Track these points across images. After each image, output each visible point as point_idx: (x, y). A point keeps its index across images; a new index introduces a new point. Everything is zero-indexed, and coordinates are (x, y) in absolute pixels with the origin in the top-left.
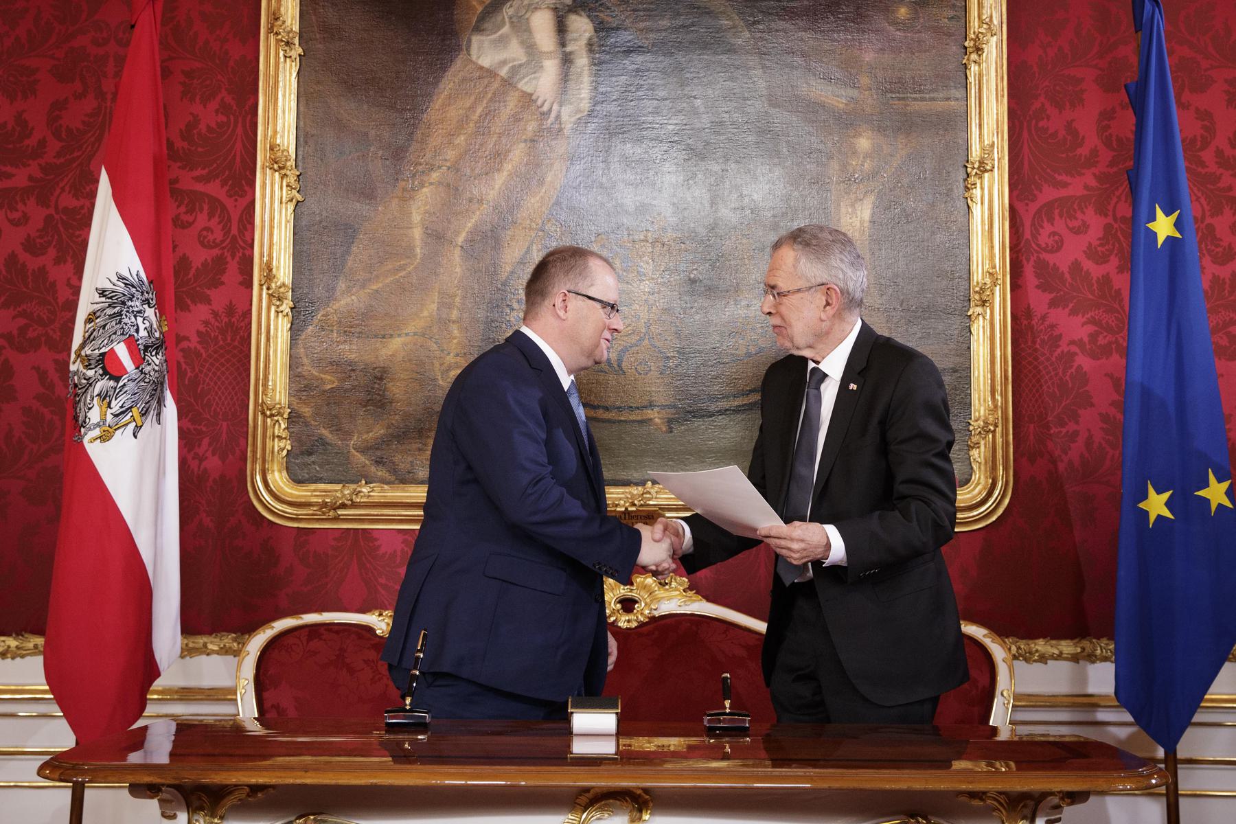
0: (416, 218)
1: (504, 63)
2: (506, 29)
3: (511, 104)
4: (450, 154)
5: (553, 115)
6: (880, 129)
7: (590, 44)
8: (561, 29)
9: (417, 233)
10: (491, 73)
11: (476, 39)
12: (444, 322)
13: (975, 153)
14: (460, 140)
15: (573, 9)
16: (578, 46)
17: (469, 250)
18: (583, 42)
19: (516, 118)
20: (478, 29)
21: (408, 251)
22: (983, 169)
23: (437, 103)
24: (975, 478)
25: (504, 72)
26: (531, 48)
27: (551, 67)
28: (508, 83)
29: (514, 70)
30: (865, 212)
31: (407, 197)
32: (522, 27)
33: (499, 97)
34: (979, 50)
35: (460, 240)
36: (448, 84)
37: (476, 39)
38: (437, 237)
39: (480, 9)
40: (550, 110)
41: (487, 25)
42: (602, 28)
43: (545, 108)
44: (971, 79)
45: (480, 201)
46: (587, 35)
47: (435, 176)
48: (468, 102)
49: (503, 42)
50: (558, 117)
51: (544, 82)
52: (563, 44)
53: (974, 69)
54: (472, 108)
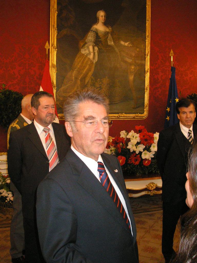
0: (73, 75)
1: (85, 53)
2: (86, 48)
3: (87, 59)
5: (92, 61)
7: (97, 51)
9: (74, 78)
10: (83, 55)
11: (82, 49)
14: (80, 64)
15: (95, 46)
16: (96, 52)
18: (96, 51)
20: (82, 48)
21: (72, 80)
23: (76, 58)
24: (145, 113)
25: (86, 55)
26: (89, 51)
27: (92, 54)
28: (86, 56)
29: (87, 54)
32: (88, 48)
35: (80, 79)
36: (78, 55)
37: (82, 49)
38: (76, 78)
39: (82, 45)
40: (92, 61)
42: (99, 49)
43: (91, 60)
44: (146, 59)
45: (82, 73)
46: (97, 50)
47: (76, 69)
48: (80, 59)
49: (85, 50)
50: (93, 61)
51: (91, 56)
54: (81, 60)
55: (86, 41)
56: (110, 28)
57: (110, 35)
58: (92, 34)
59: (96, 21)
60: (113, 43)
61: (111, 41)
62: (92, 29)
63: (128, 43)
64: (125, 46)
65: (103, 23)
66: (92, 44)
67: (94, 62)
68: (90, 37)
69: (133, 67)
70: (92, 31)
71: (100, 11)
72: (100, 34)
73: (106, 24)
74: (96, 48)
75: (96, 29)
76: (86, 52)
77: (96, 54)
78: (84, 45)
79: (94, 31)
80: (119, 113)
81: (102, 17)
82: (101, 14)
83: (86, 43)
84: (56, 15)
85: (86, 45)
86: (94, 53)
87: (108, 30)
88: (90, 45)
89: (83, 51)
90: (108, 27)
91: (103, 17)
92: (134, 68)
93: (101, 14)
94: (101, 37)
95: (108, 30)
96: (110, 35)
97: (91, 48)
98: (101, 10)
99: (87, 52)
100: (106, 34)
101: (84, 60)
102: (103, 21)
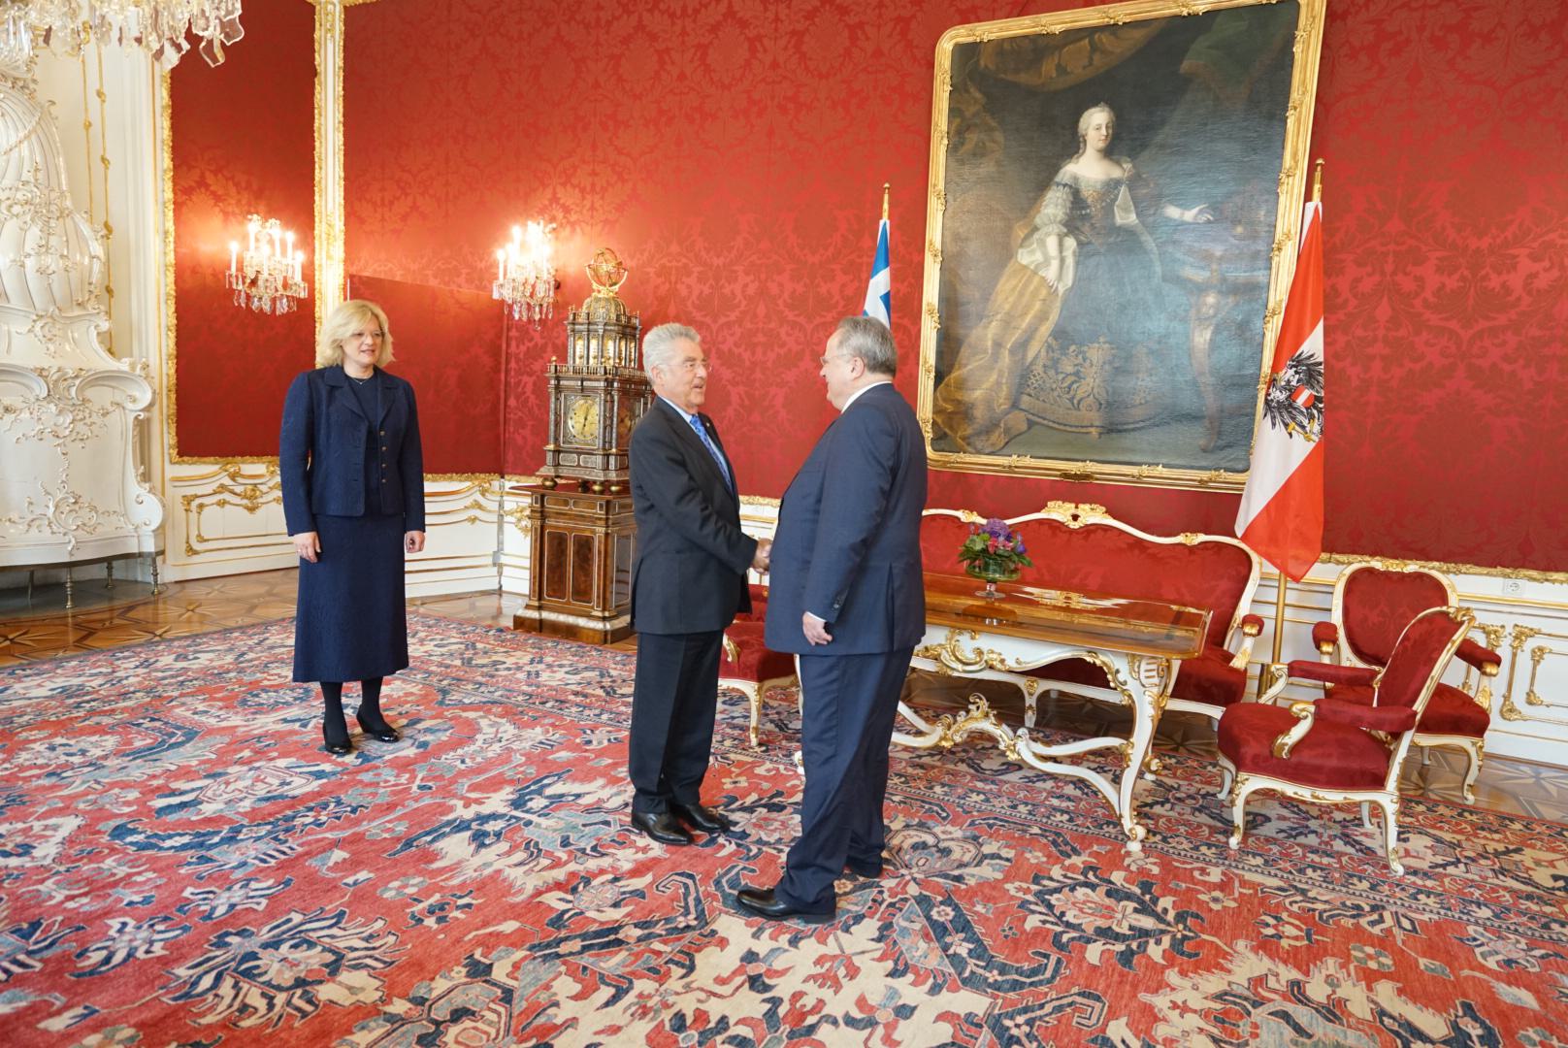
0: (990, 336)
3: (1036, 281)
4: (1007, 307)
6: (1220, 292)
8: (1061, 245)
9: (989, 343)
10: (1025, 267)
11: (1020, 251)
12: (998, 383)
13: (1271, 305)
15: (1066, 235)
16: (1069, 254)
17: (1012, 352)
19: (1037, 290)
20: (1021, 246)
21: (985, 351)
22: (1274, 313)
27: (1055, 264)
28: (1035, 273)
29: (1037, 266)
30: (1208, 335)
31: (986, 327)
32: (1042, 243)
33: (1029, 281)
34: (1279, 249)
38: (998, 345)
41: (1027, 243)
42: (1080, 244)
47: (999, 317)
48: (1014, 282)
49: (1032, 252)
52: (1061, 251)
53: (1275, 260)
55: (1038, 221)
56: (1127, 166)
57: (1123, 189)
58: (1058, 194)
59: (1073, 146)
60: (1132, 218)
61: (1126, 210)
62: (1058, 179)
63: (1195, 211)
64: (1183, 223)
65: (1099, 151)
66: (1056, 228)
67: (1061, 290)
68: (1053, 206)
69: (1211, 299)
70: (1058, 184)
71: (1092, 110)
72: (1087, 193)
73: (1109, 152)
74: (1071, 243)
75: (1076, 178)
76: (1033, 258)
77: (1070, 261)
78: (1027, 237)
79: (1065, 185)
80: (1140, 464)
81: (1098, 129)
82: (1096, 122)
83: (1036, 229)
84: (943, 149)
85: (1036, 236)
86: (1062, 260)
87: (1116, 173)
88: (1048, 234)
89: (1025, 257)
90: (1118, 163)
91: (1104, 131)
92: (1218, 303)
93: (1096, 122)
94: (1089, 201)
95: (1116, 173)
96: (1123, 189)
97: (1052, 242)
98: (1095, 104)
99: (1038, 257)
100: (1112, 186)
101: (1026, 286)
102: (1101, 145)
